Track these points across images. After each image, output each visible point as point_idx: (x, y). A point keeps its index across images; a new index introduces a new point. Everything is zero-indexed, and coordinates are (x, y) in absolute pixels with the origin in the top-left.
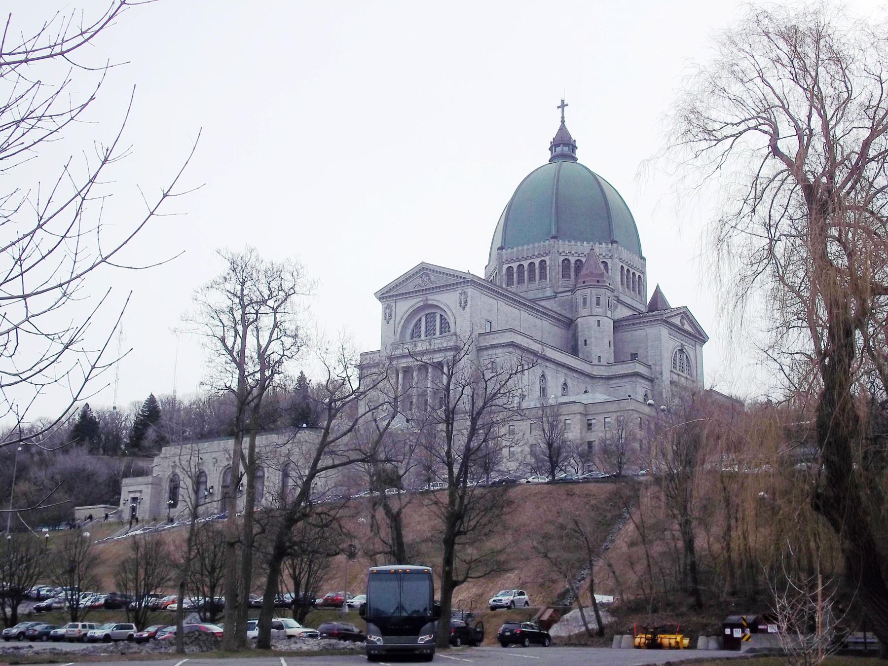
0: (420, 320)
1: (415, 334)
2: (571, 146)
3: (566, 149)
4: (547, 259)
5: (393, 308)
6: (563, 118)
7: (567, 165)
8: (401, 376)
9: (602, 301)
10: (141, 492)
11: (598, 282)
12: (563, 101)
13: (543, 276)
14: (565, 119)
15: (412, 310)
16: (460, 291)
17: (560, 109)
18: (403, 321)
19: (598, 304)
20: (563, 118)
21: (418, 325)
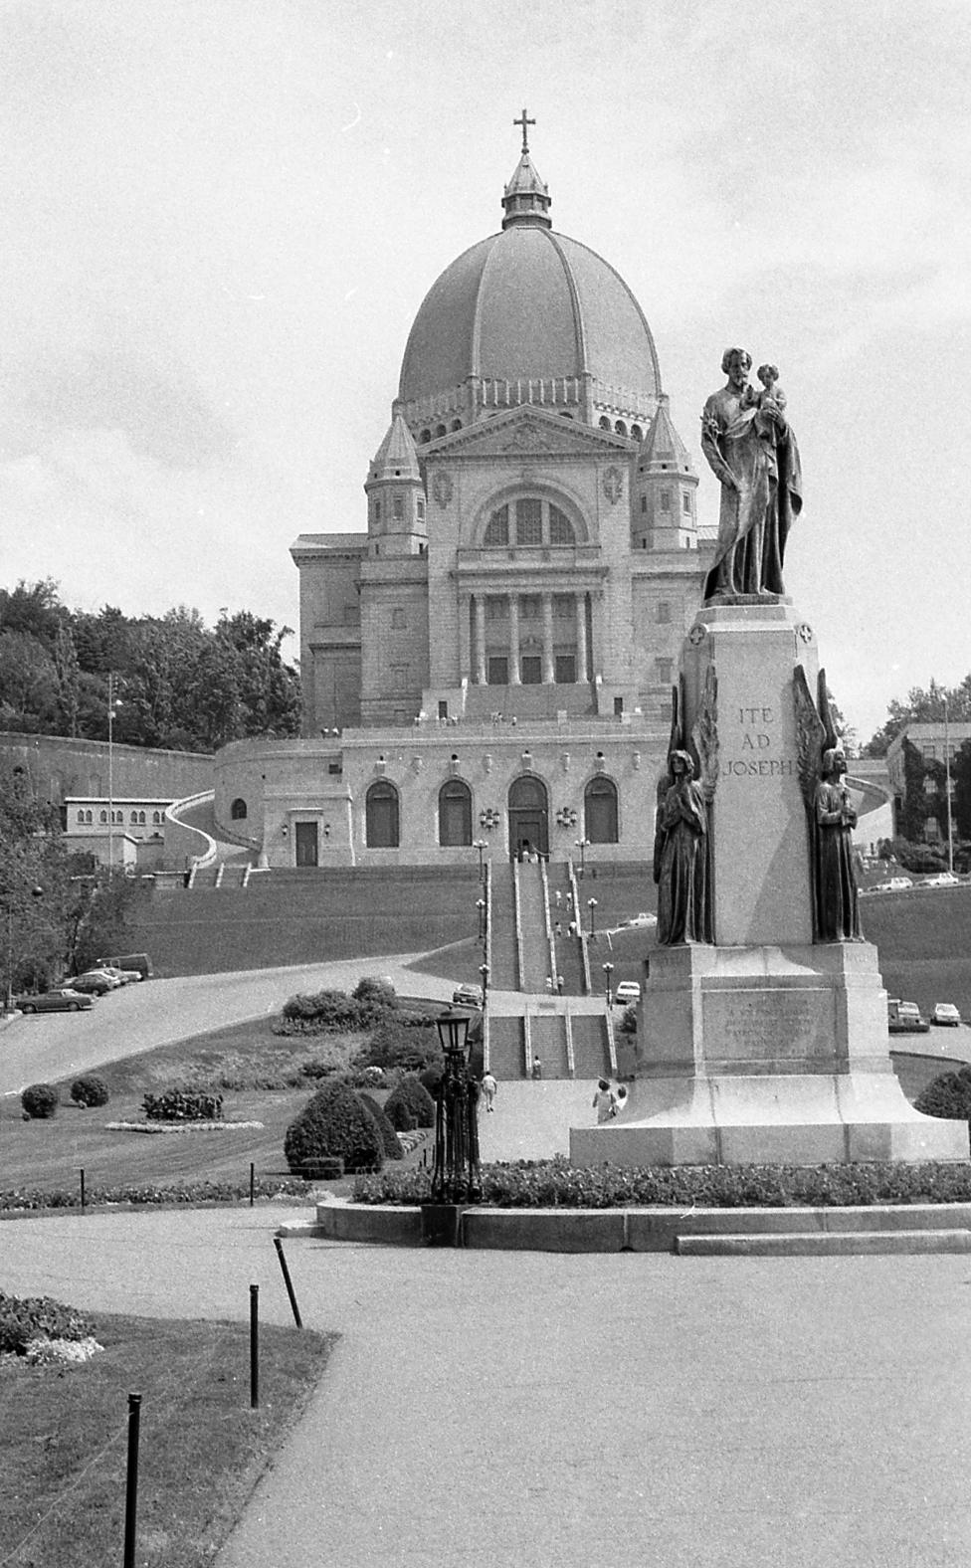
0: (507, 506)
1: (496, 534)
4: (574, 411)
5: (454, 481)
6: (525, 144)
7: (531, 234)
8: (480, 609)
14: (528, 147)
17: (521, 126)
20: (525, 144)
21: (500, 517)
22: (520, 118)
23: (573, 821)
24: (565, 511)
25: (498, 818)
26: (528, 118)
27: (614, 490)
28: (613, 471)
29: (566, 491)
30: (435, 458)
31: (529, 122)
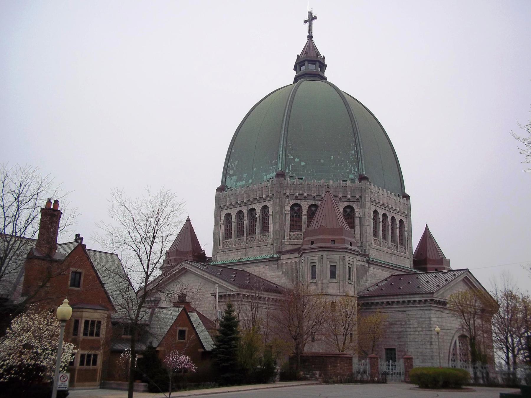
2: (318, 64)
3: (312, 67)
6: (310, 32)
9: (339, 272)
11: (333, 241)
12: (310, 14)
13: (265, 228)
14: (314, 34)
19: (333, 275)
20: (310, 32)
26: (313, 15)
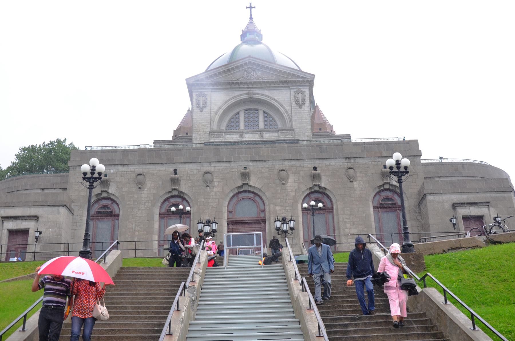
5: (208, 97)
6: (251, 15)
10: (36, 218)
12: (251, 4)
15: (233, 101)
16: (295, 90)
17: (249, 9)
18: (221, 111)
20: (251, 15)
22: (249, 6)
23: (292, 229)
24: (271, 113)
25: (214, 226)
27: (300, 101)
28: (298, 92)
29: (273, 102)
30: (198, 85)
31: (253, 8)
